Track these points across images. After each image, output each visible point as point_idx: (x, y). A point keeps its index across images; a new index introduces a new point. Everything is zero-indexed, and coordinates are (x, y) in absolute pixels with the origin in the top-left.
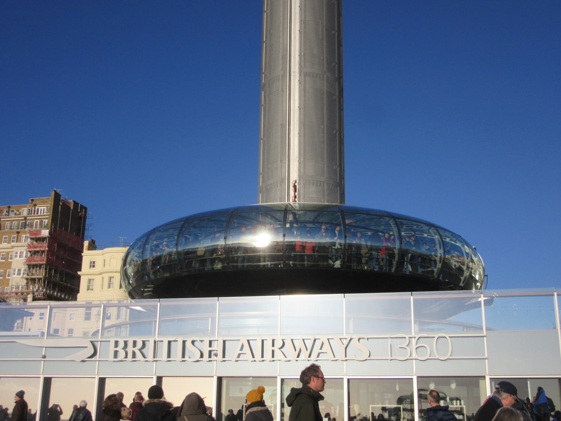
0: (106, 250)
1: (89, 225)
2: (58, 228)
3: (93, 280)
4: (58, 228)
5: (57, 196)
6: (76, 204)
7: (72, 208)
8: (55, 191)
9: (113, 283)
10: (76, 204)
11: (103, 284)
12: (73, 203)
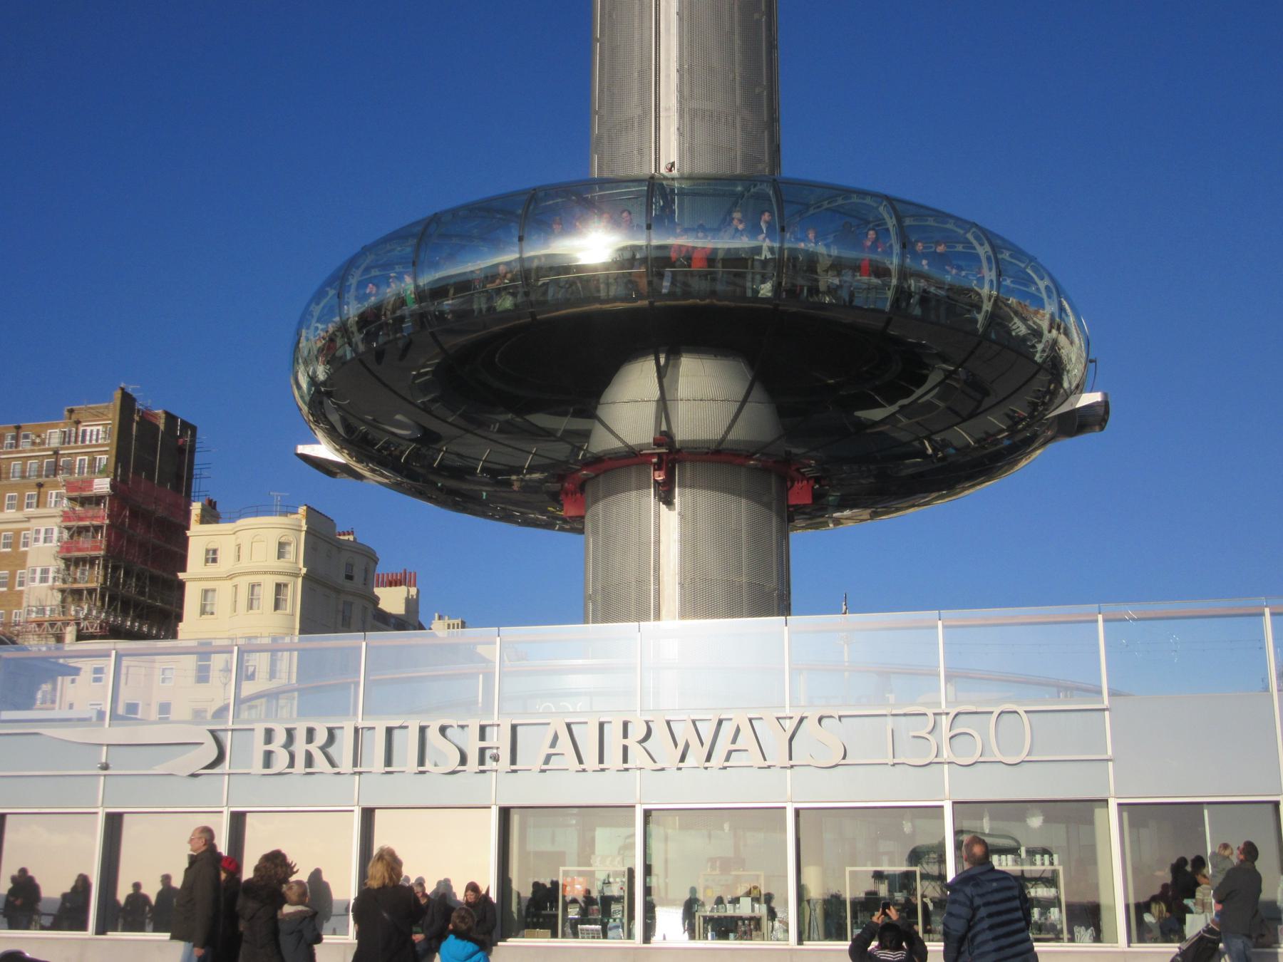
0: (243, 522)
1: (200, 467)
2: (131, 476)
3: (214, 590)
4: (131, 476)
5: (128, 402)
6: (171, 418)
7: (162, 427)
8: (123, 389)
9: (259, 599)
10: (171, 418)
11: (236, 601)
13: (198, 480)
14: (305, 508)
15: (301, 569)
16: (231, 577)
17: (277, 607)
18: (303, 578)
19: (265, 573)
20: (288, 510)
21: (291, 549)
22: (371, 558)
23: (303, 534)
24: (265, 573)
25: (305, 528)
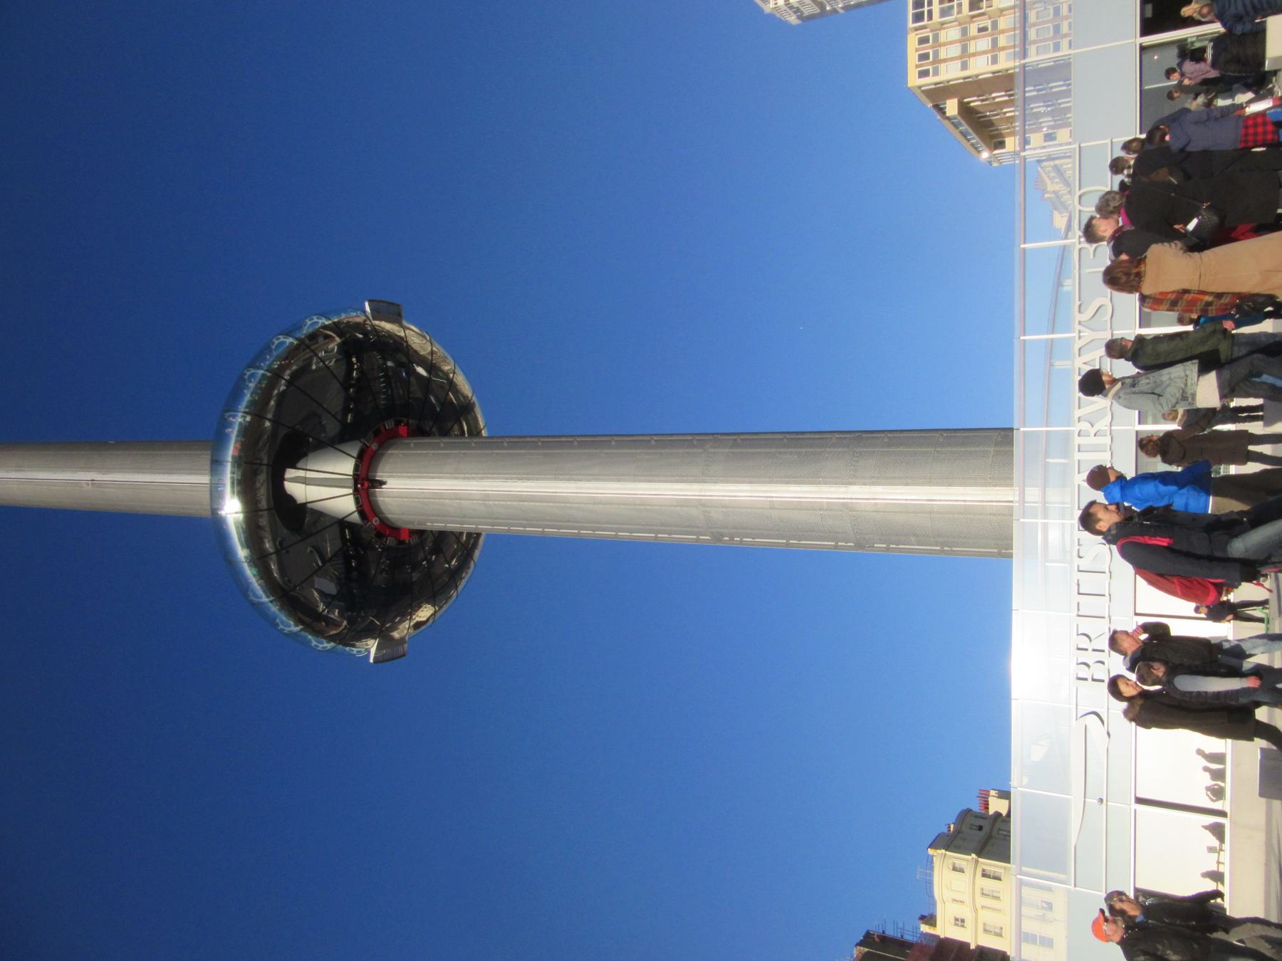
1: (896, 930)
3: (984, 924)
6: (861, 944)
7: (866, 950)
9: (992, 891)
10: (861, 944)
12: (858, 947)
13: (906, 932)
14: (929, 849)
15: (973, 858)
16: (976, 910)
17: (999, 879)
18: (979, 857)
19: (974, 883)
20: (930, 861)
21: (958, 863)
22: (967, 812)
23: (948, 853)
24: (974, 883)
25: (943, 851)
